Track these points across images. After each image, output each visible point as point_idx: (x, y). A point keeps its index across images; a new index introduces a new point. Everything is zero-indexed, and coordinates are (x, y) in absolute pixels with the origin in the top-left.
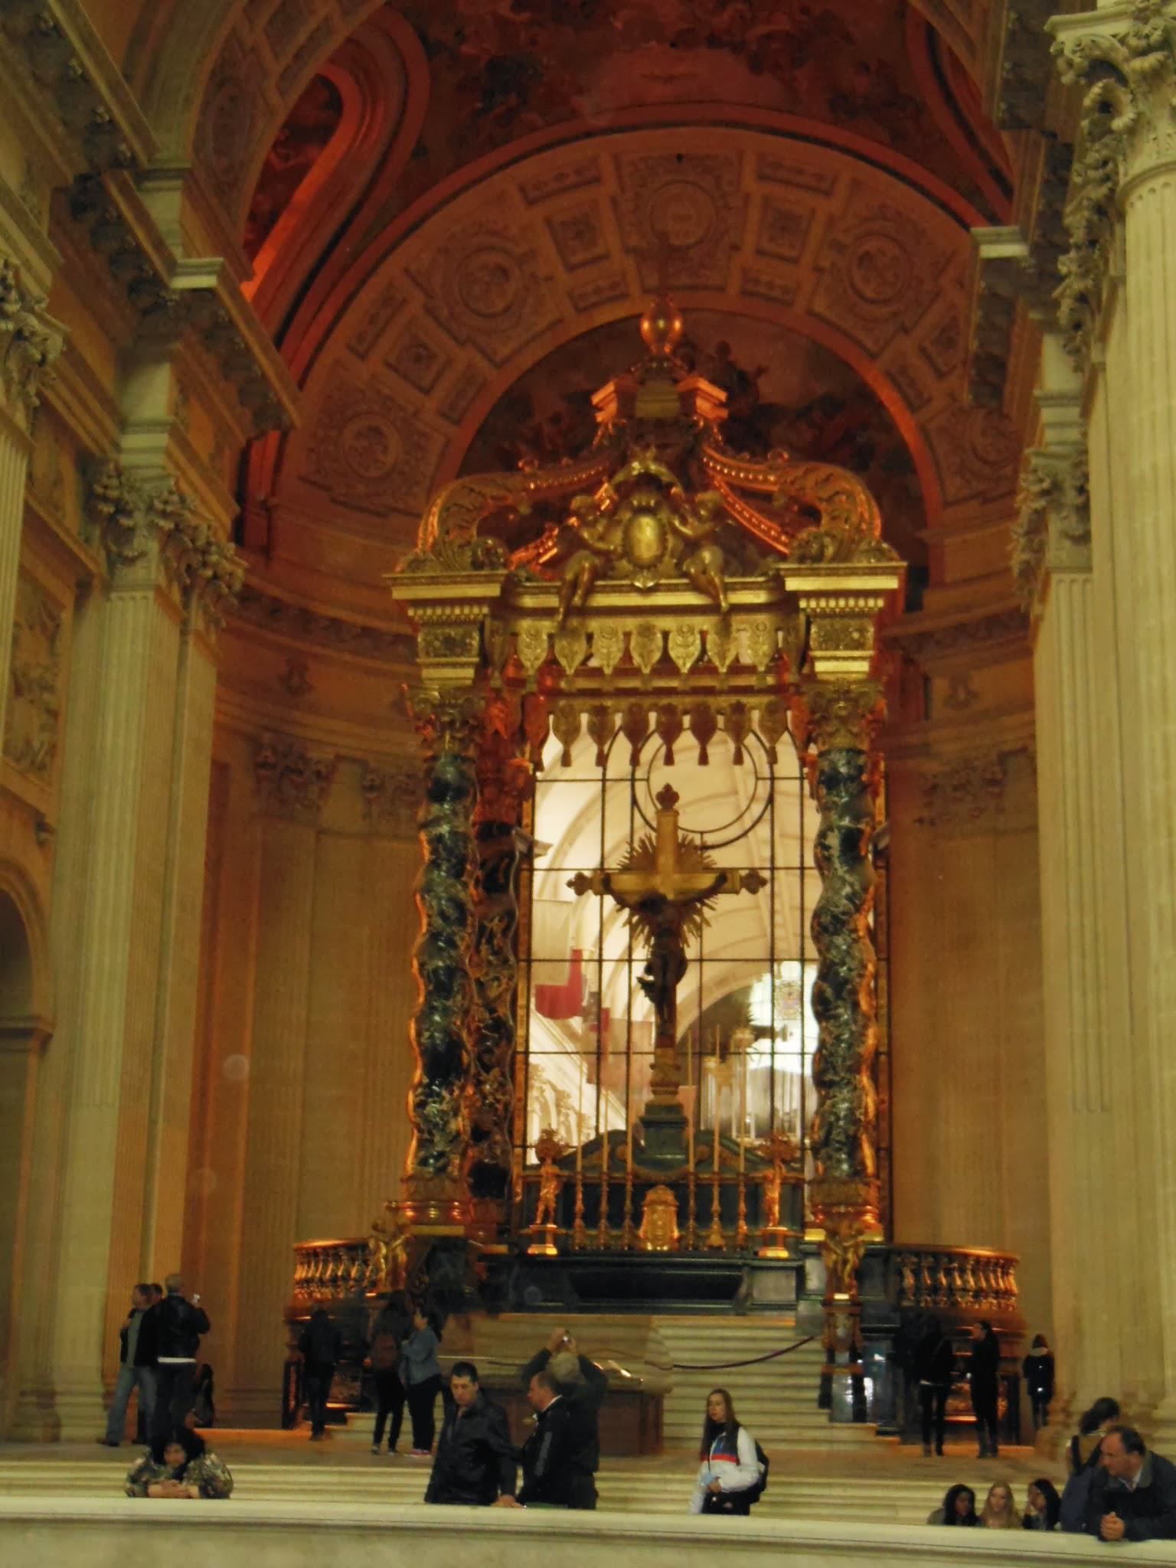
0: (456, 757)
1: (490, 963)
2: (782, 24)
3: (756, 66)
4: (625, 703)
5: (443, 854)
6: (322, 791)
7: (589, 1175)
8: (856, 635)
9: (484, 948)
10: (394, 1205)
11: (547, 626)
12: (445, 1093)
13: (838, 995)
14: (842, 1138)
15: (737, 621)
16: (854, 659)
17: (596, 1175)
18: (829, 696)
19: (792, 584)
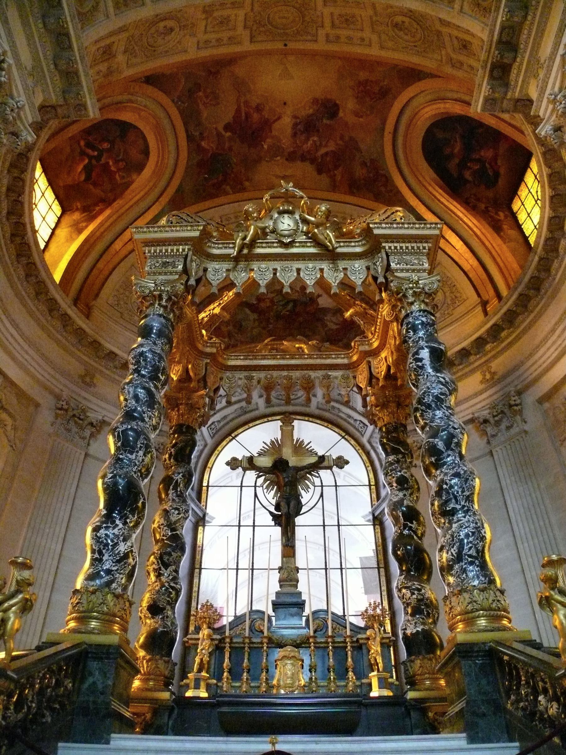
0: (160, 315)
1: (173, 500)
2: (332, 147)
3: (320, 172)
4: (262, 375)
5: (143, 363)
6: (92, 435)
7: (235, 640)
8: (416, 262)
9: (171, 492)
10: (20, 560)
11: (226, 266)
12: (118, 522)
13: (448, 445)
14: (473, 552)
15: (342, 264)
16: (419, 271)
17: (240, 640)
18: (407, 286)
19: (376, 232)
